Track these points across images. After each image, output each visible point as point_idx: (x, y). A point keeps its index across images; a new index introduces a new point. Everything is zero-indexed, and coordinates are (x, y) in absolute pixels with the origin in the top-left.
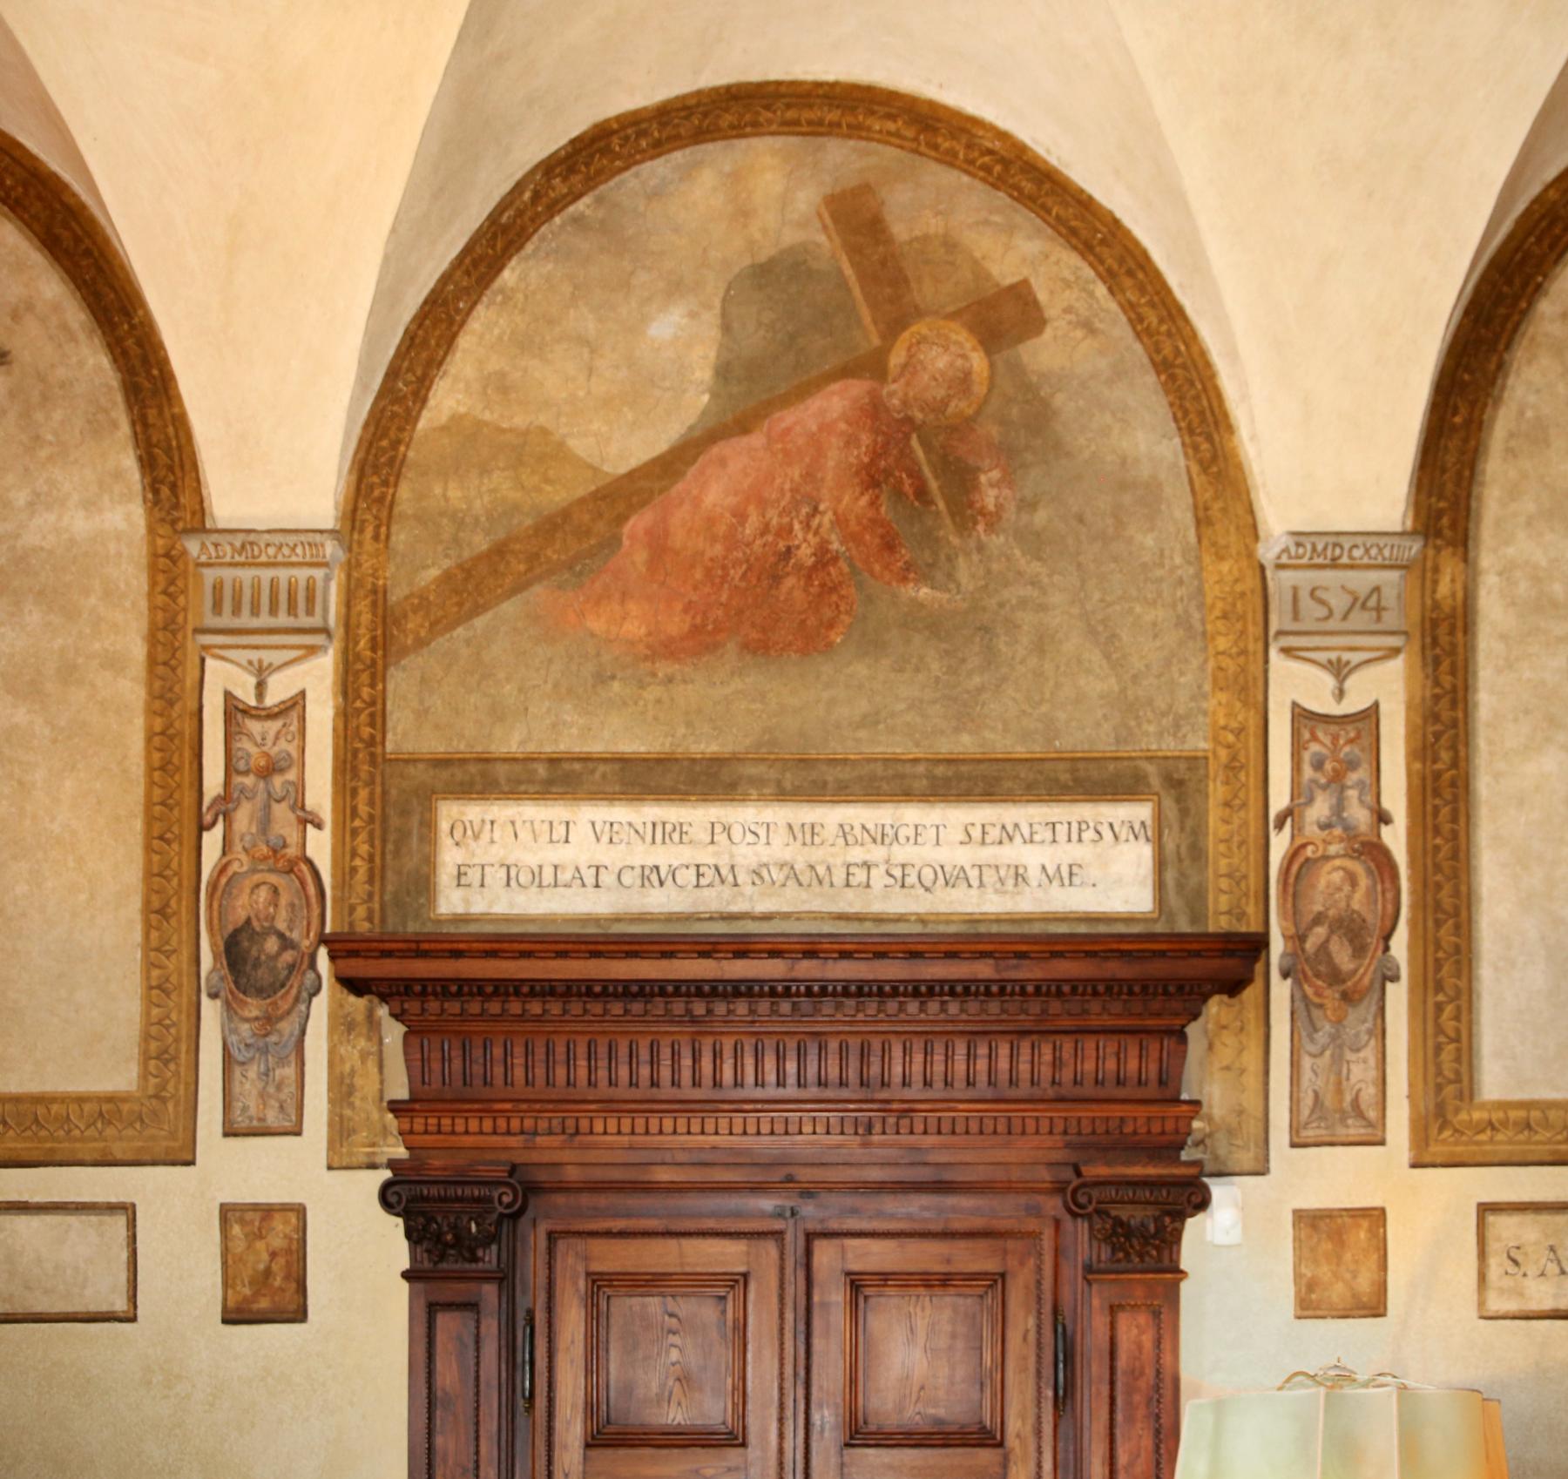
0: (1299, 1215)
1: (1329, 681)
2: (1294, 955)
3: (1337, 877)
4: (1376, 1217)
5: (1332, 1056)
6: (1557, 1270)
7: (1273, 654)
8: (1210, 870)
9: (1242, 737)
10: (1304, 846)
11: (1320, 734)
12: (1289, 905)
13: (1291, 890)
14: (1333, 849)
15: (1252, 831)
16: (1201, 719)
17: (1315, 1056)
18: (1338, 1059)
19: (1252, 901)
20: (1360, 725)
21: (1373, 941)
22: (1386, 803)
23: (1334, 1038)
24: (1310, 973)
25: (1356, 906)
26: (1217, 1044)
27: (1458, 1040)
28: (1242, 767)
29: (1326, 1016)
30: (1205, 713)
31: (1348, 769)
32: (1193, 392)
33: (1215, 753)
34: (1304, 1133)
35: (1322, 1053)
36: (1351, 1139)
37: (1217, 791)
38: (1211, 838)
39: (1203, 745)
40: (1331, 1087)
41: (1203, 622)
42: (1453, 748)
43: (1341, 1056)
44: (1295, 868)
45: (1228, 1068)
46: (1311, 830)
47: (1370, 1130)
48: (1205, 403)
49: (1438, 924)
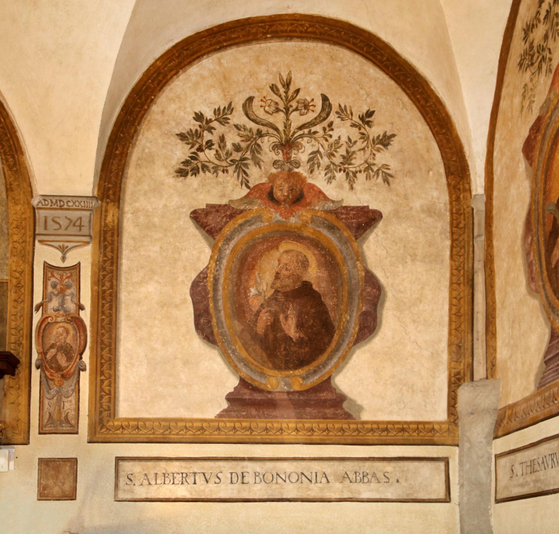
0: (41, 460)
1: (60, 254)
2: (42, 360)
3: (61, 330)
4: (74, 461)
5: (57, 399)
6: (148, 483)
7: (37, 243)
8: (8, 326)
9: (23, 275)
10: (47, 318)
11: (55, 275)
12: (40, 341)
13: (41, 335)
14: (59, 319)
15: (26, 312)
16: (5, 267)
17: (50, 399)
18: (59, 401)
19: (25, 338)
20: (72, 271)
21: (75, 355)
22: (82, 302)
23: (58, 392)
24: (48, 367)
25: (68, 341)
26: (8, 393)
27: (110, 394)
28: (23, 286)
29: (55, 384)
30: (7, 265)
31: (66, 288)
32: (7, 138)
33: (11, 281)
34: (45, 429)
35: (53, 398)
36: (64, 431)
37: (12, 295)
38: (8, 314)
39: (6, 277)
40: (56, 411)
41: (8, 229)
42: (111, 281)
43: (61, 399)
44: (43, 326)
45: (13, 403)
46: (50, 312)
47: (72, 428)
48: (12, 143)
49: (102, 349)
